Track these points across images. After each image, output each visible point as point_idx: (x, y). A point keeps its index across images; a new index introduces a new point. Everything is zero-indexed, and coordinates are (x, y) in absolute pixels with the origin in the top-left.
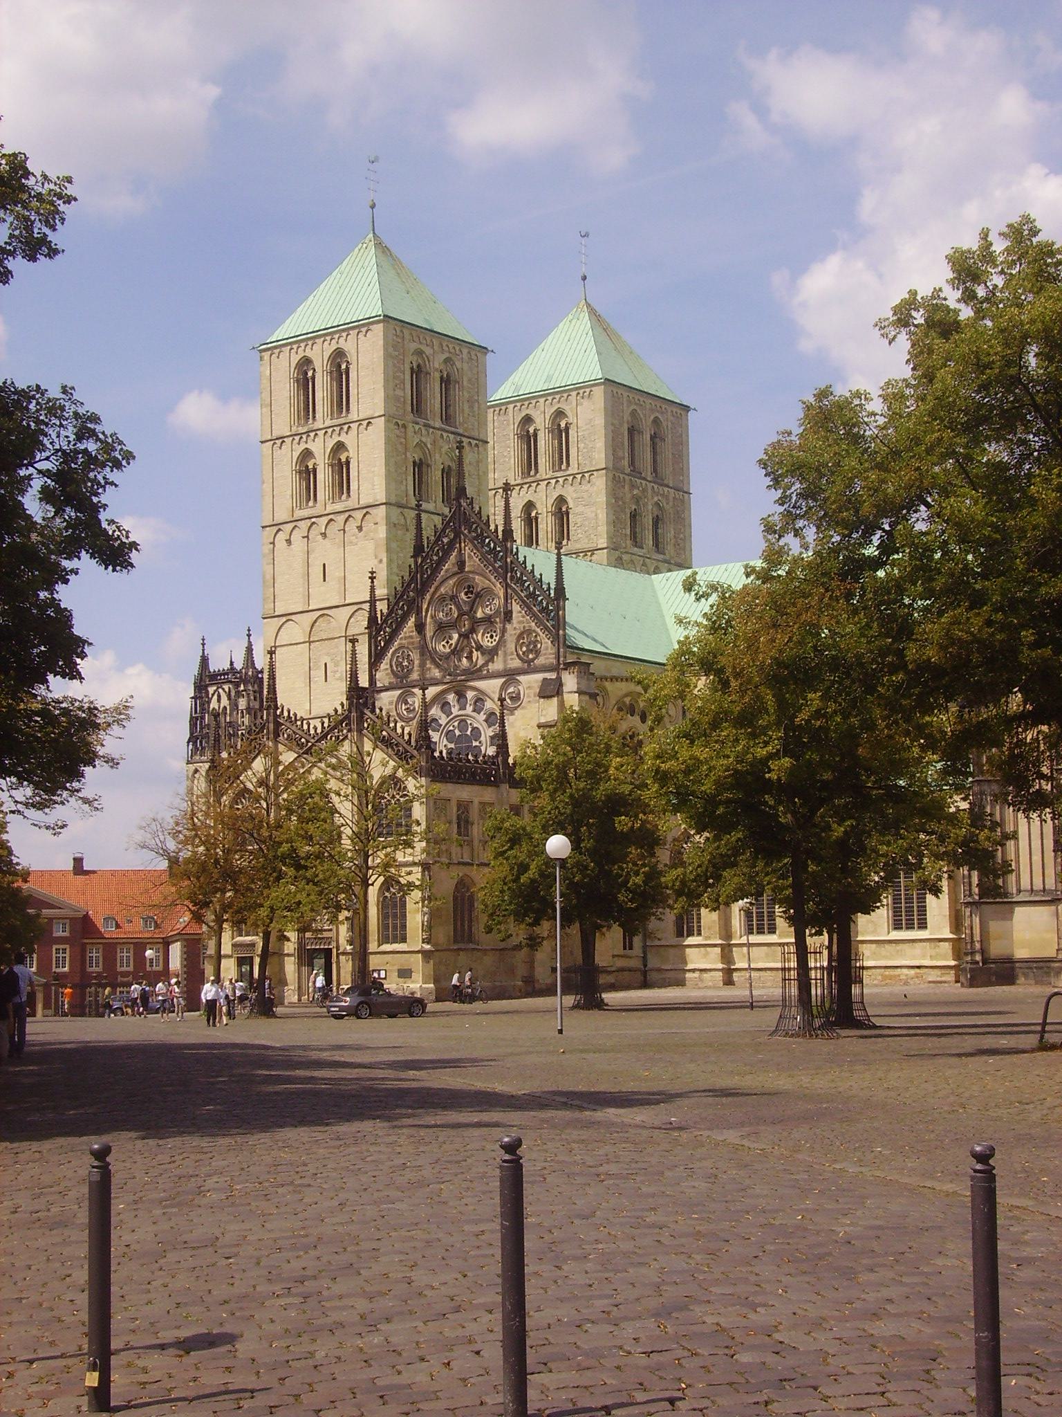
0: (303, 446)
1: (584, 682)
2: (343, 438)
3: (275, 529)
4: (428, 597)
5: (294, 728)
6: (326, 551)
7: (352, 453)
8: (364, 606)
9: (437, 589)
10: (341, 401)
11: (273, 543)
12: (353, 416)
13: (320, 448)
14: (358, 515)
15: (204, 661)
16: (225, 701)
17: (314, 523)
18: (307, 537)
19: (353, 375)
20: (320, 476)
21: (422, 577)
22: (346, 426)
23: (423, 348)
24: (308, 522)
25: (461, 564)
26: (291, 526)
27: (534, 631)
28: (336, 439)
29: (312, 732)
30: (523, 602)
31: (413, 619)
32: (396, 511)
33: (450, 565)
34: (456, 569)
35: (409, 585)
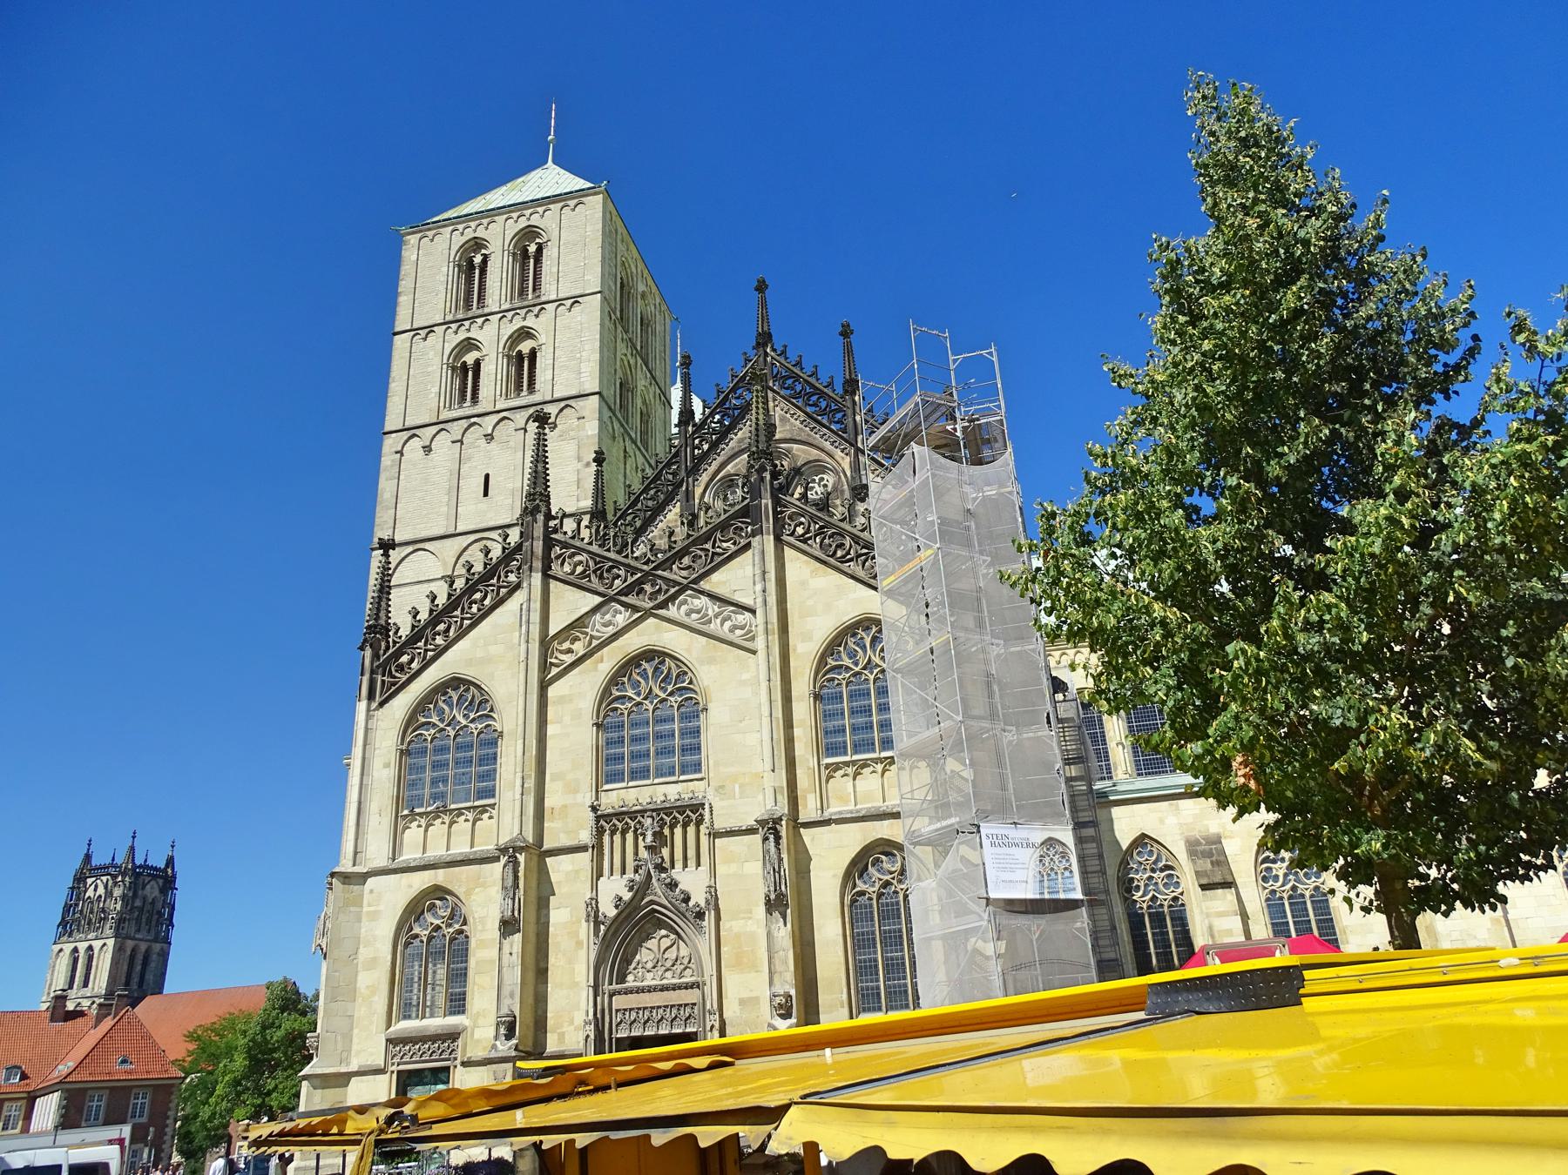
0: (462, 335)
2: (530, 322)
3: (406, 435)
4: (705, 478)
7: (542, 339)
11: (401, 453)
13: (491, 338)
15: (88, 857)
16: (101, 890)
17: (475, 423)
18: (461, 442)
19: (549, 255)
20: (487, 370)
22: (540, 307)
26: (434, 429)
31: (677, 510)
32: (607, 413)
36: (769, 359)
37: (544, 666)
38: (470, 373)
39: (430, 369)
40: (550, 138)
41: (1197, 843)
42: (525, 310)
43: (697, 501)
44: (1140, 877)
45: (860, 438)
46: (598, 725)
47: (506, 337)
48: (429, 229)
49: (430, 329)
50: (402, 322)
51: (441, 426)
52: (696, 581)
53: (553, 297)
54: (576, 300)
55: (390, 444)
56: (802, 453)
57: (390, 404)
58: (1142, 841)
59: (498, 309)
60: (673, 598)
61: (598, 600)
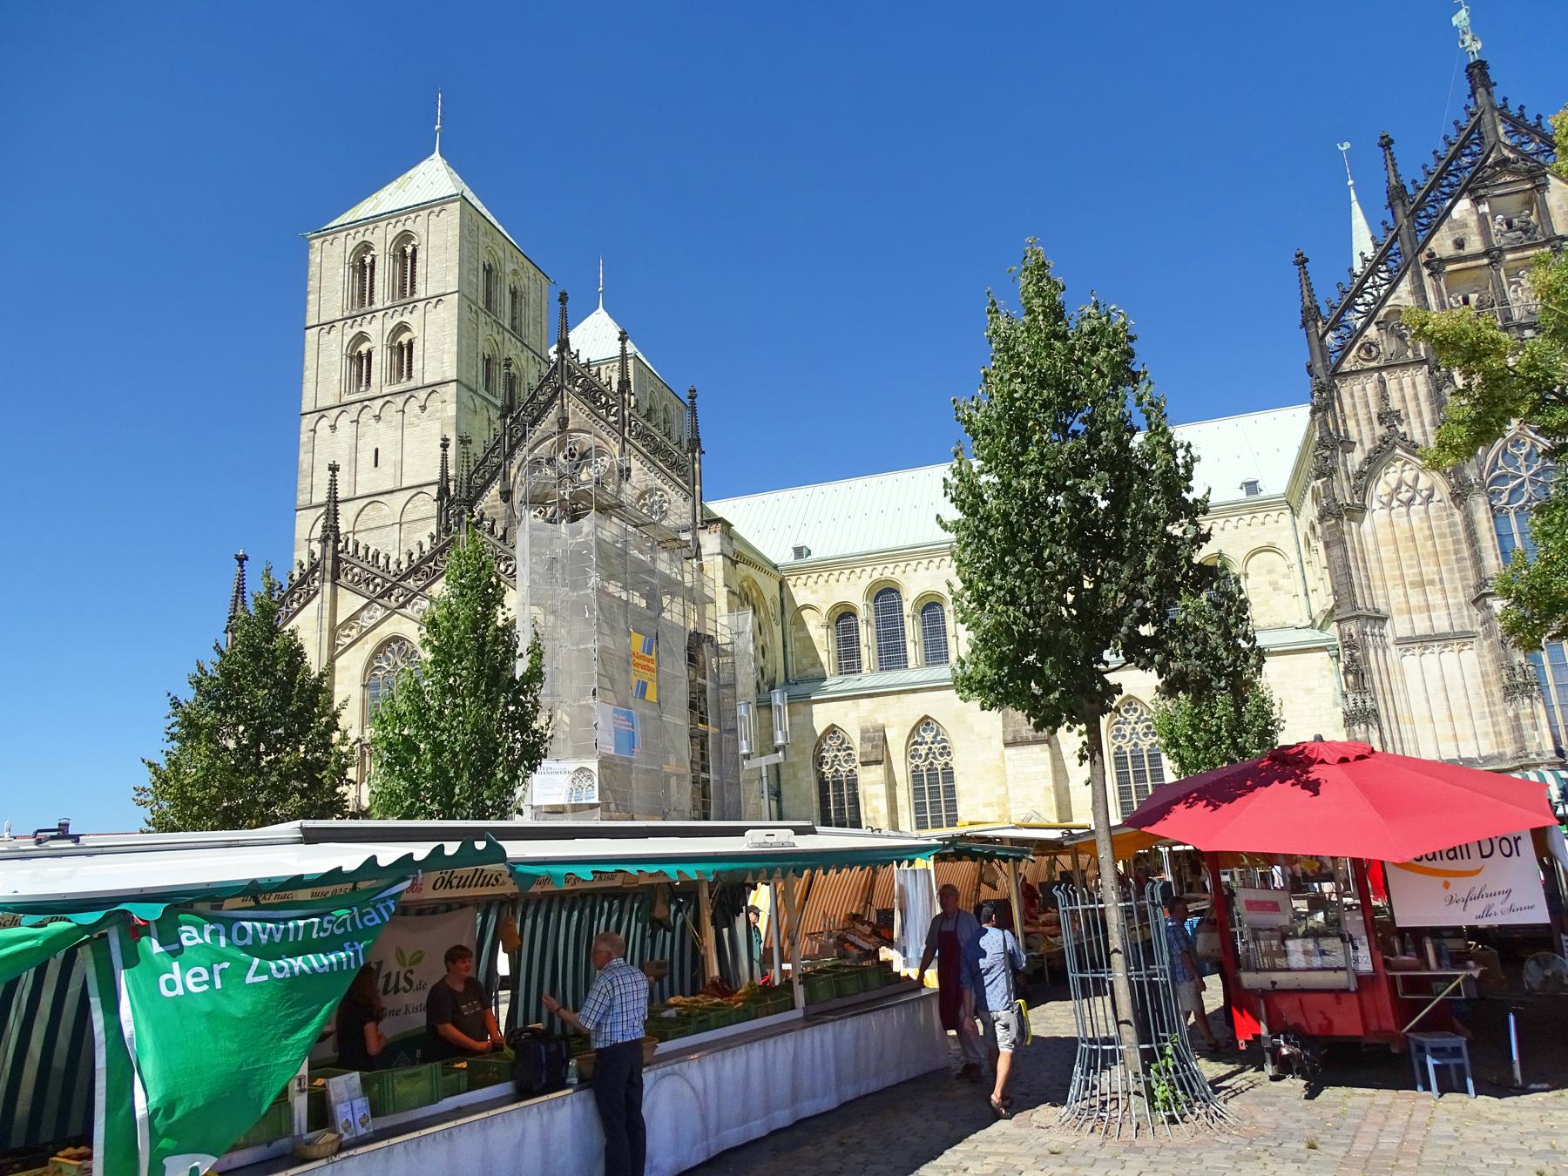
0: (356, 330)
1: (727, 546)
3: (317, 416)
5: (364, 564)
6: (378, 434)
7: (416, 331)
8: (425, 489)
9: (531, 450)
10: (405, 285)
11: (314, 431)
12: (420, 294)
13: (377, 330)
14: (423, 394)
17: (366, 406)
18: (357, 422)
19: (421, 256)
20: (376, 359)
21: (510, 440)
23: (496, 248)
24: (359, 406)
25: (563, 422)
26: (337, 411)
27: (660, 490)
28: (397, 319)
29: (392, 567)
30: (646, 456)
32: (466, 394)
33: (549, 422)
34: (556, 428)
35: (493, 450)
36: (565, 362)
37: (333, 646)
38: (365, 361)
39: (333, 359)
40: (437, 127)
41: (868, 731)
42: (402, 308)
43: (512, 480)
44: (828, 756)
45: (627, 429)
46: (364, 686)
47: (388, 331)
48: (329, 234)
49: (332, 324)
50: (311, 321)
51: (343, 408)
52: (423, 590)
53: (423, 296)
54: (439, 298)
55: (307, 423)
56: (588, 440)
57: (304, 390)
58: (832, 730)
59: (381, 307)
60: (409, 601)
61: (366, 601)
